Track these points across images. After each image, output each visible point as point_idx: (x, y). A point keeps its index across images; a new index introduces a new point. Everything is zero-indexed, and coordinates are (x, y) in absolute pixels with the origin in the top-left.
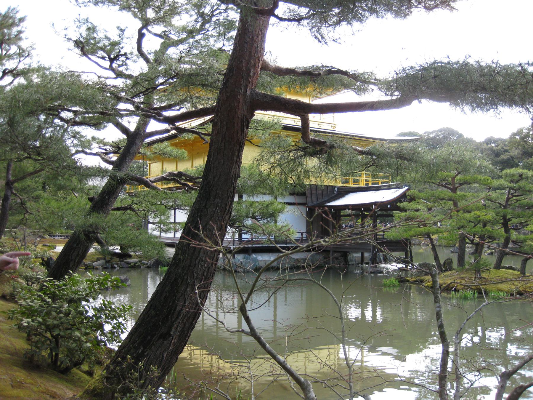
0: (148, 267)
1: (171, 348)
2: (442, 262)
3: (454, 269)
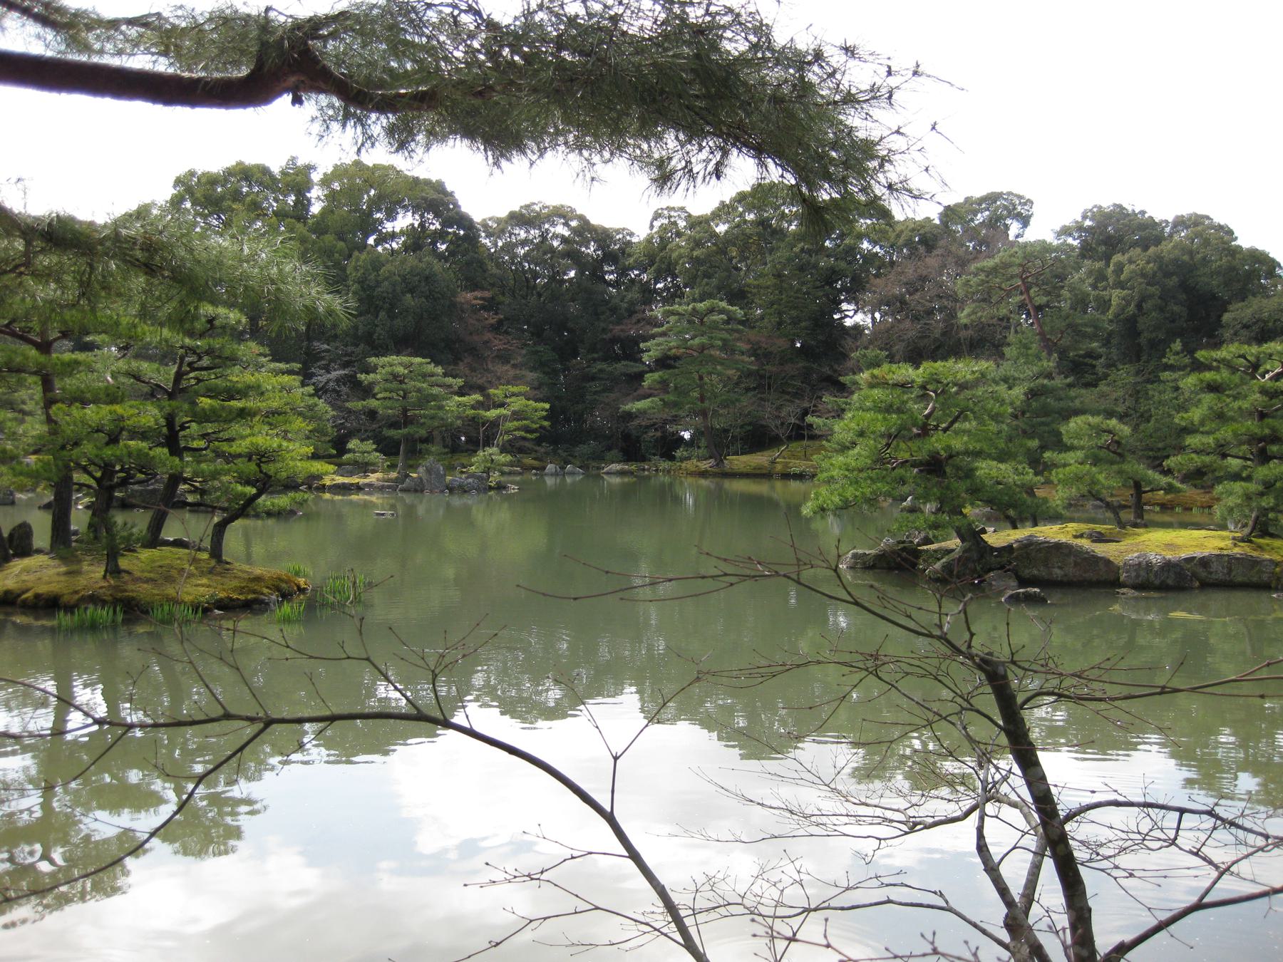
3: (39, 551)
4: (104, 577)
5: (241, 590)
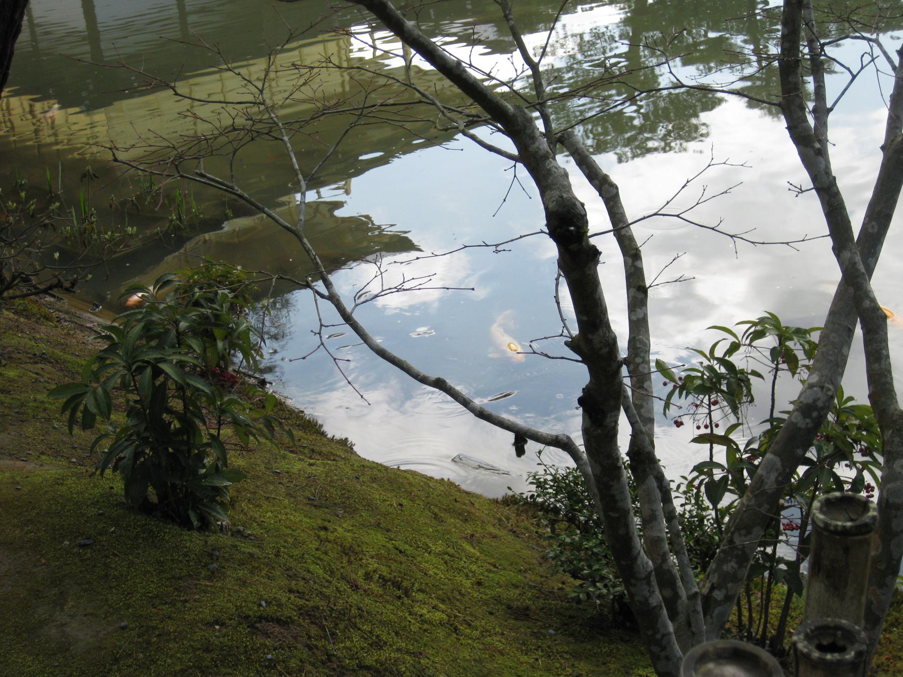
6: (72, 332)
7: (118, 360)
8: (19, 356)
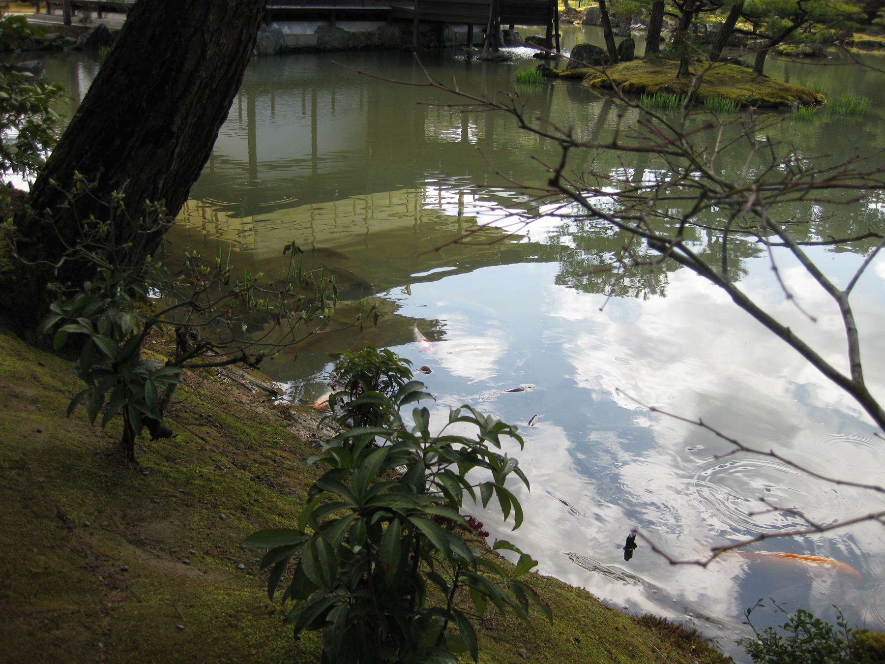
0: (78, 49)
1: (174, 167)
2: (617, 47)
3: (637, 58)
4: (678, 76)
5: (772, 95)
6: (229, 388)
7: (345, 498)
8: (186, 415)
